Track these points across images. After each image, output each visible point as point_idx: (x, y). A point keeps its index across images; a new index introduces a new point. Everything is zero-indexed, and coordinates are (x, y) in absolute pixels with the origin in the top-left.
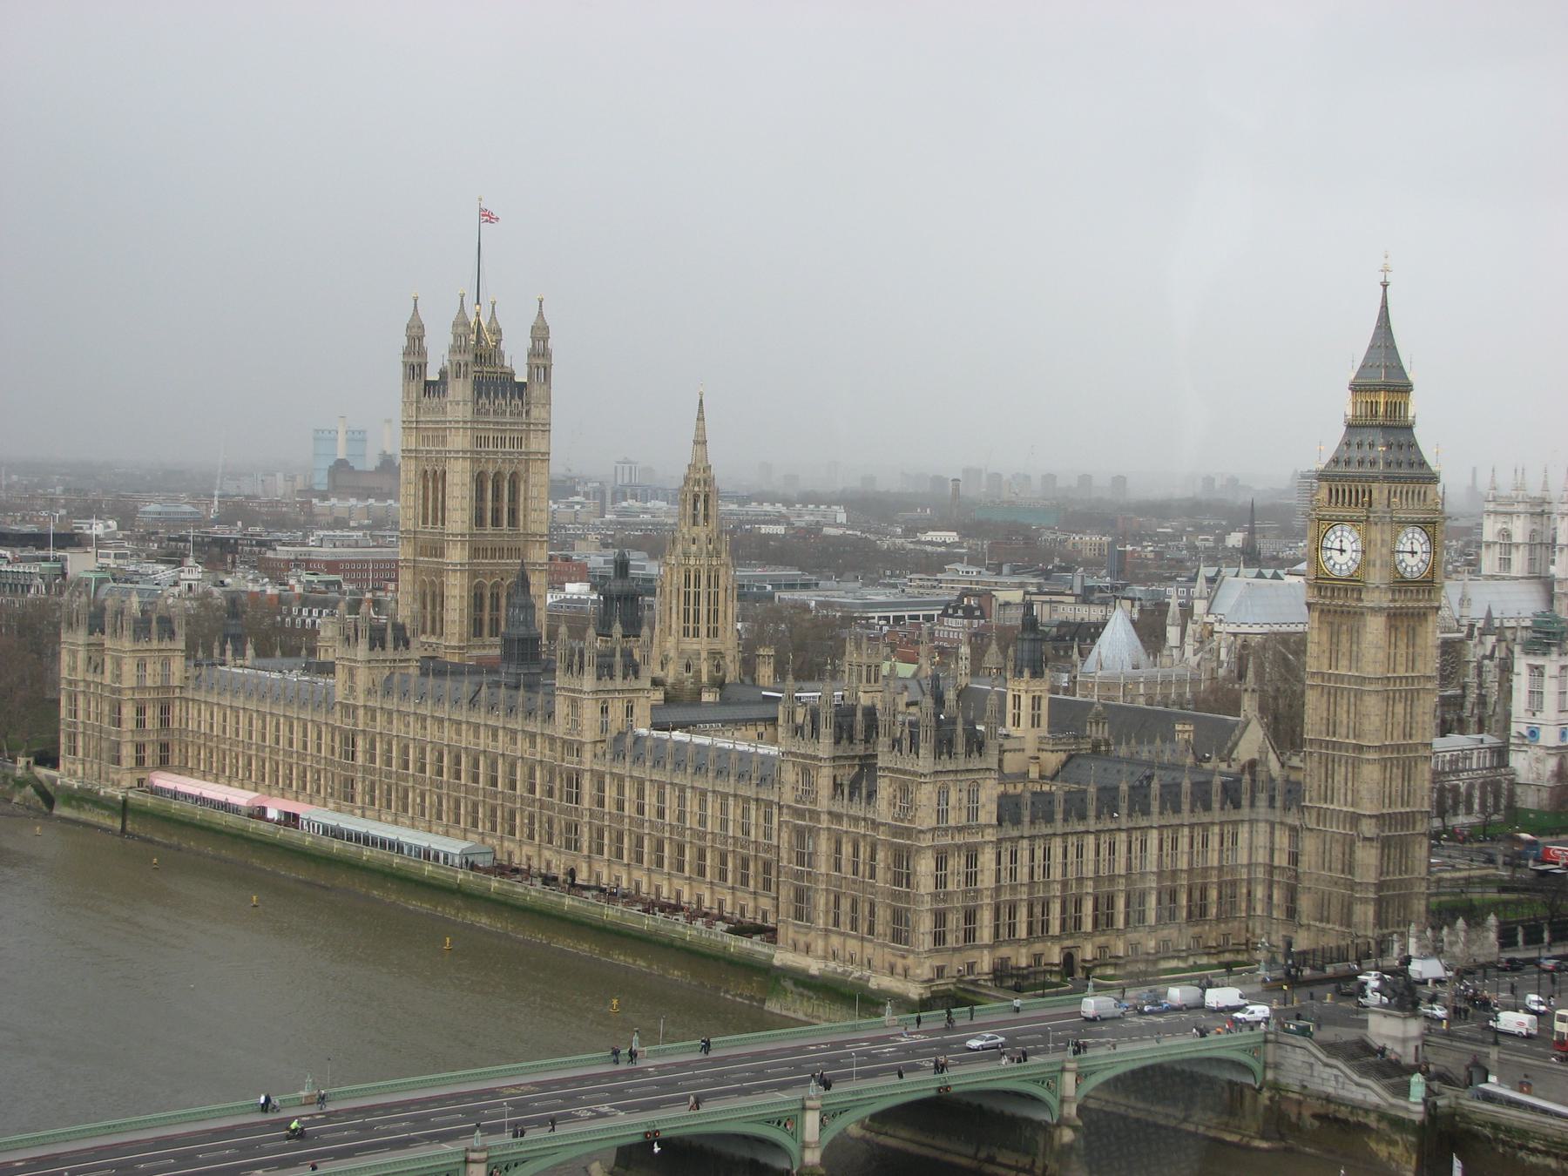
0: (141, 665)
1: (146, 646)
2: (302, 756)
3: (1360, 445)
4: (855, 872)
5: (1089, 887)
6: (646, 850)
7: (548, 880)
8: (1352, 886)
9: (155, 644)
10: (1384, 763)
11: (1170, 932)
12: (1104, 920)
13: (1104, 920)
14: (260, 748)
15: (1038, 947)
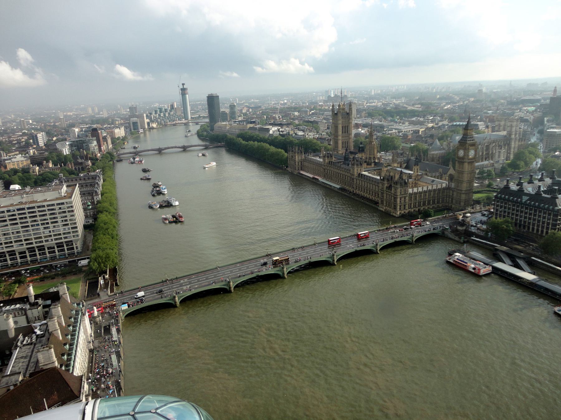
0: (298, 157)
5: (422, 200)
7: (350, 192)
8: (460, 199)
11: (434, 205)
12: (424, 204)
13: (424, 204)
15: (414, 209)
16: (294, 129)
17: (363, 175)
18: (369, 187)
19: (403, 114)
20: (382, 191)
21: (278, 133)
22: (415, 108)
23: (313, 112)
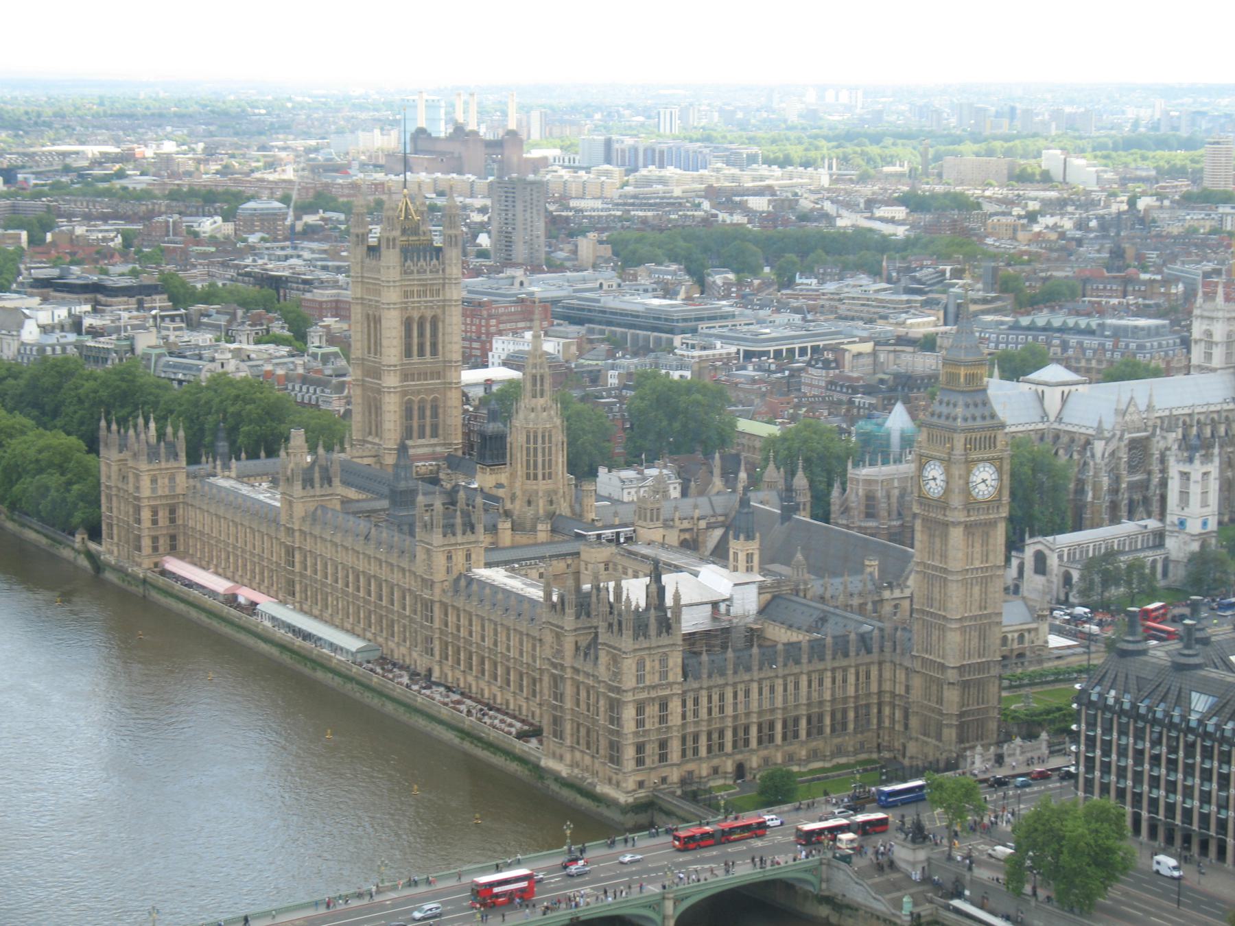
0: (154, 481)
1: (157, 467)
2: (261, 558)
3: (948, 404)
4: (588, 710)
5: (754, 719)
6: (474, 663)
7: (414, 675)
8: (941, 713)
9: (163, 465)
10: (963, 630)
11: (817, 744)
12: (766, 737)
13: (766, 737)
14: (235, 547)
15: (716, 762)
16: (173, 318)
17: (475, 587)
18: (501, 648)
19: (792, 257)
20: (555, 666)
21: (72, 337)
22: (877, 225)
23: (310, 219)
